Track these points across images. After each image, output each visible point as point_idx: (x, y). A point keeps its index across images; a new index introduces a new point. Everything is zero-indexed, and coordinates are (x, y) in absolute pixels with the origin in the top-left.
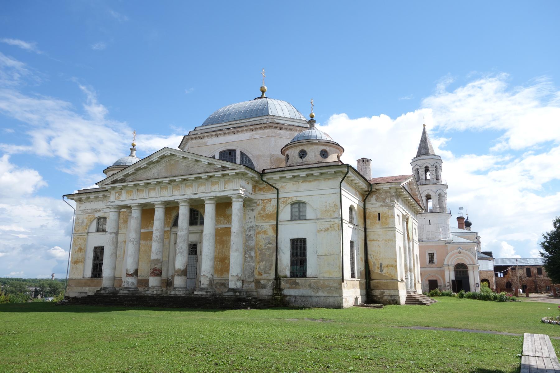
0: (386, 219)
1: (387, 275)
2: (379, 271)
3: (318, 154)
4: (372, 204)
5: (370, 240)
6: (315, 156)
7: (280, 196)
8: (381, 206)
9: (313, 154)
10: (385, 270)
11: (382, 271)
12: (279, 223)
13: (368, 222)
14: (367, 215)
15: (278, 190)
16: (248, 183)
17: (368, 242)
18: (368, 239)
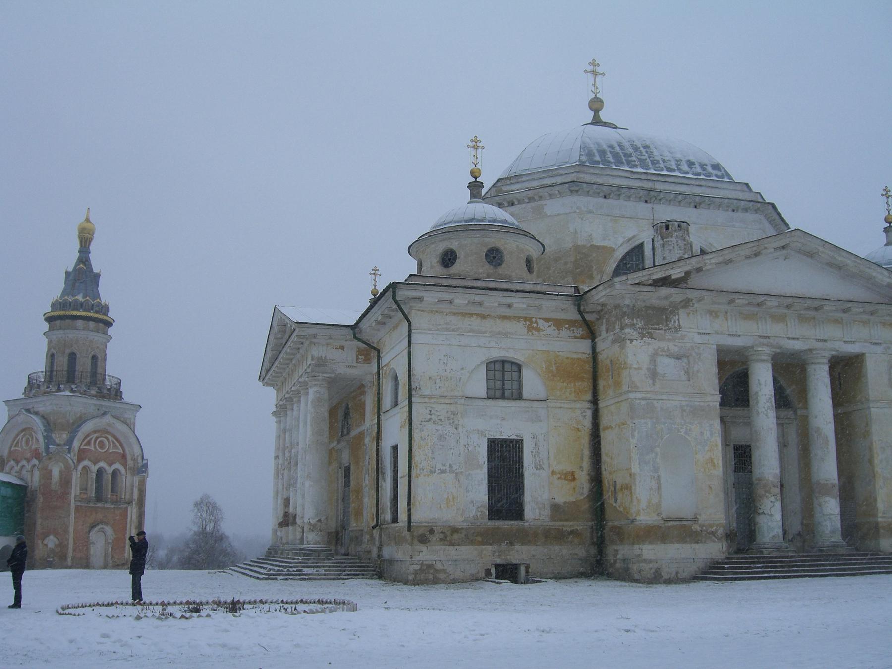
0: (619, 374)
1: (622, 510)
2: (612, 501)
3: (435, 260)
4: (604, 340)
5: (607, 428)
6: (432, 267)
7: (384, 361)
8: (614, 342)
9: (429, 265)
10: (620, 495)
11: (616, 502)
12: (383, 417)
13: (601, 383)
14: (600, 366)
15: (379, 351)
16: (342, 348)
17: (602, 434)
18: (601, 427)
